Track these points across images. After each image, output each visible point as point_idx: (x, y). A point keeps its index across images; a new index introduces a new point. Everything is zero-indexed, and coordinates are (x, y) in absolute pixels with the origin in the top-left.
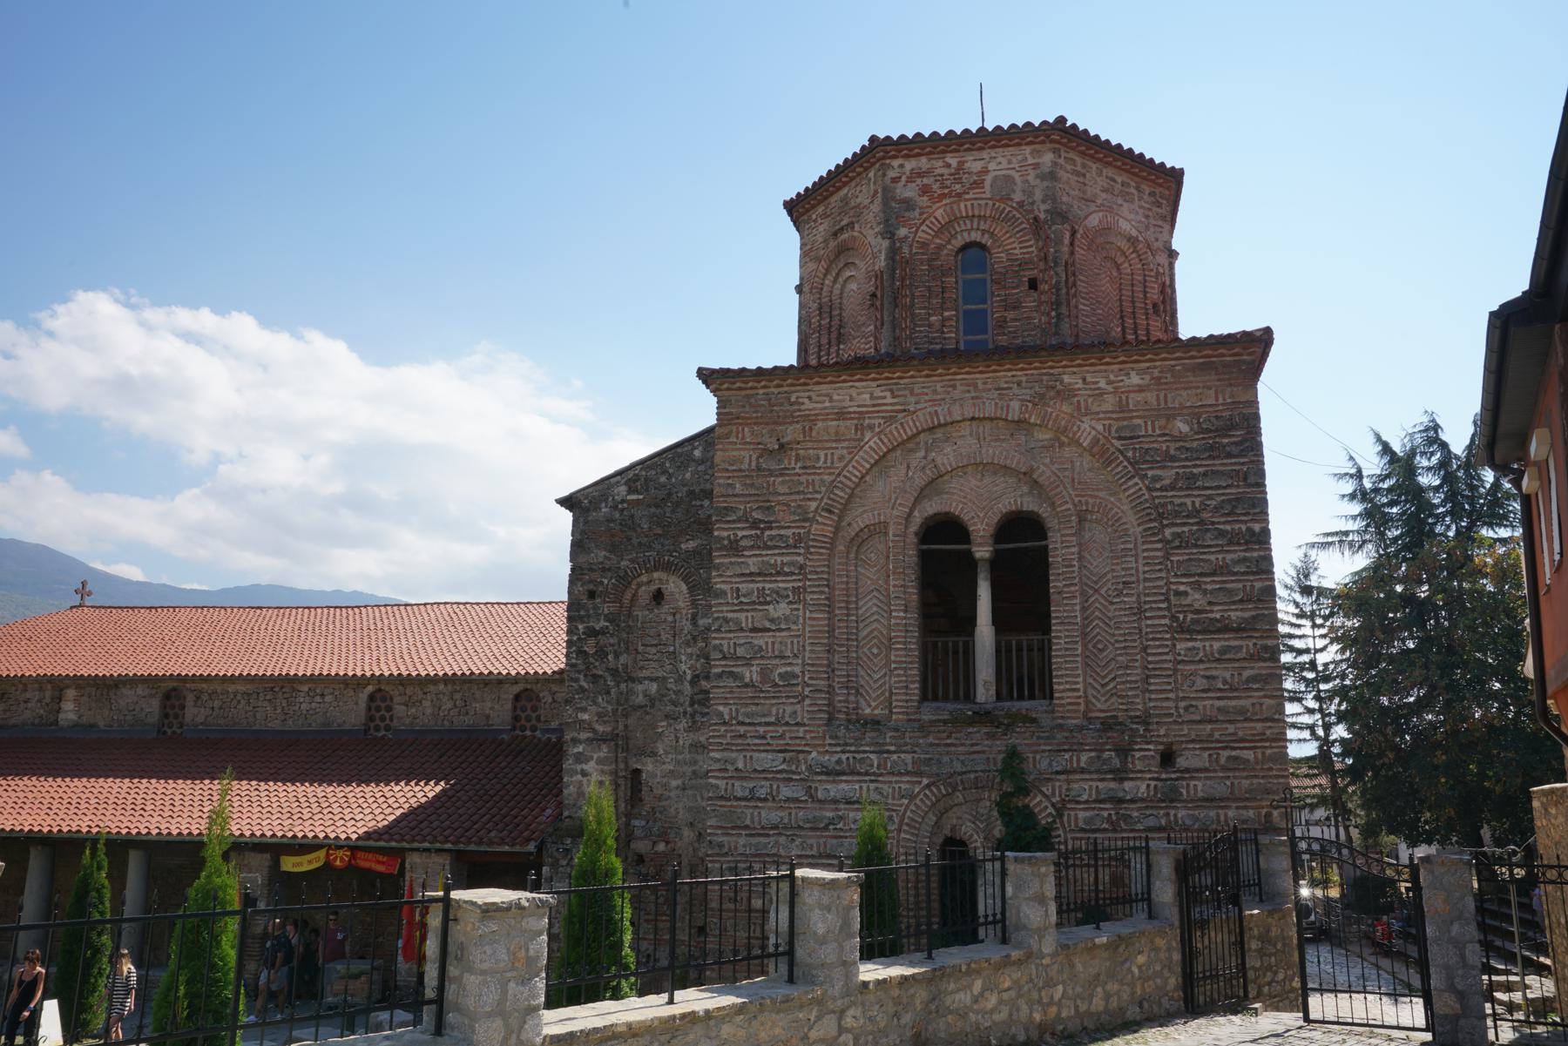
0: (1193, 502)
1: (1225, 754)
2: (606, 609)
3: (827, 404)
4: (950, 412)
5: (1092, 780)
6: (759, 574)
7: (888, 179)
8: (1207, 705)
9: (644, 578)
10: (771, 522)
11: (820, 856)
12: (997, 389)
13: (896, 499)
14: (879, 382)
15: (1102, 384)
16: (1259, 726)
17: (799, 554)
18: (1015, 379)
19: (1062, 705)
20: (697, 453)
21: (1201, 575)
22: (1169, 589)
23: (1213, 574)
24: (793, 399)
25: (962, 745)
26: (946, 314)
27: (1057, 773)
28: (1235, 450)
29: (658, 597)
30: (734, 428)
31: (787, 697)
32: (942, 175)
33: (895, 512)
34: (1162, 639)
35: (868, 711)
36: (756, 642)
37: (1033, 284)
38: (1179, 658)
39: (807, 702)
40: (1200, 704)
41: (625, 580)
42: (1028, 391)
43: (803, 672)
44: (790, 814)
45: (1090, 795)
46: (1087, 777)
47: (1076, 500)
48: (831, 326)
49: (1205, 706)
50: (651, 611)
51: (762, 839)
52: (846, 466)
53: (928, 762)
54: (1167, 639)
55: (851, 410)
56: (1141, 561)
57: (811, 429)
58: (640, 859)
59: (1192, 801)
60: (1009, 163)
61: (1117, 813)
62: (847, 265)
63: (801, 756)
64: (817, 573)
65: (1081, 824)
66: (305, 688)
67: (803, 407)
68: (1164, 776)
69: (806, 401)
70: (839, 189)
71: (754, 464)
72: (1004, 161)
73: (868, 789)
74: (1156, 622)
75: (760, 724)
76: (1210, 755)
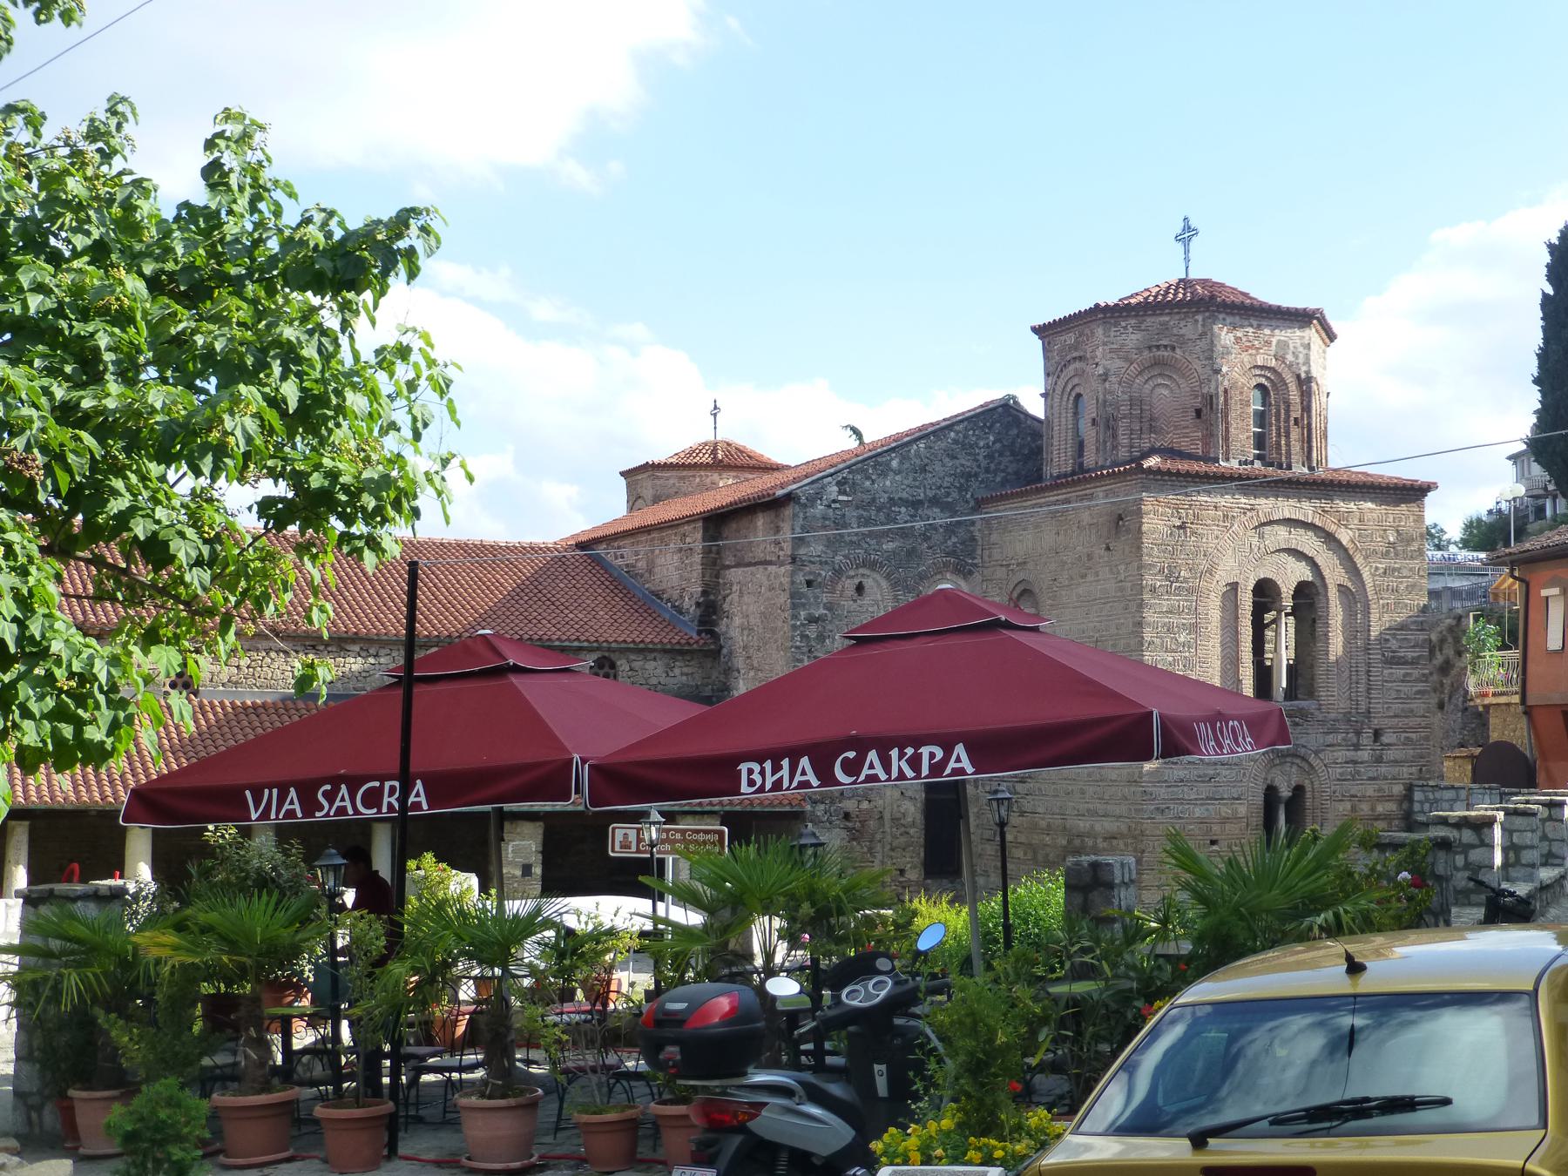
2: (825, 598)
8: (1397, 707)
9: (852, 573)
11: (1208, 798)
20: (895, 464)
29: (860, 589)
37: (1296, 419)
41: (838, 572)
50: (855, 601)
58: (847, 816)
66: (356, 648)
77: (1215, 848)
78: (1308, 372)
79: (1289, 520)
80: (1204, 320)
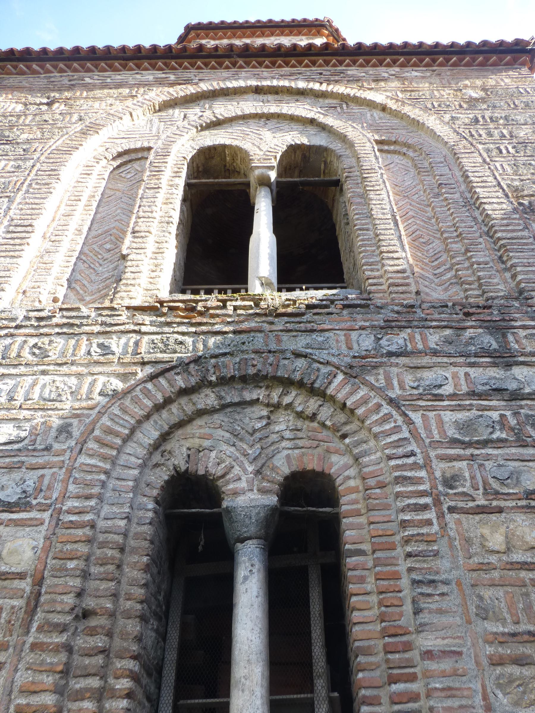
27: (390, 354)
65: (452, 432)
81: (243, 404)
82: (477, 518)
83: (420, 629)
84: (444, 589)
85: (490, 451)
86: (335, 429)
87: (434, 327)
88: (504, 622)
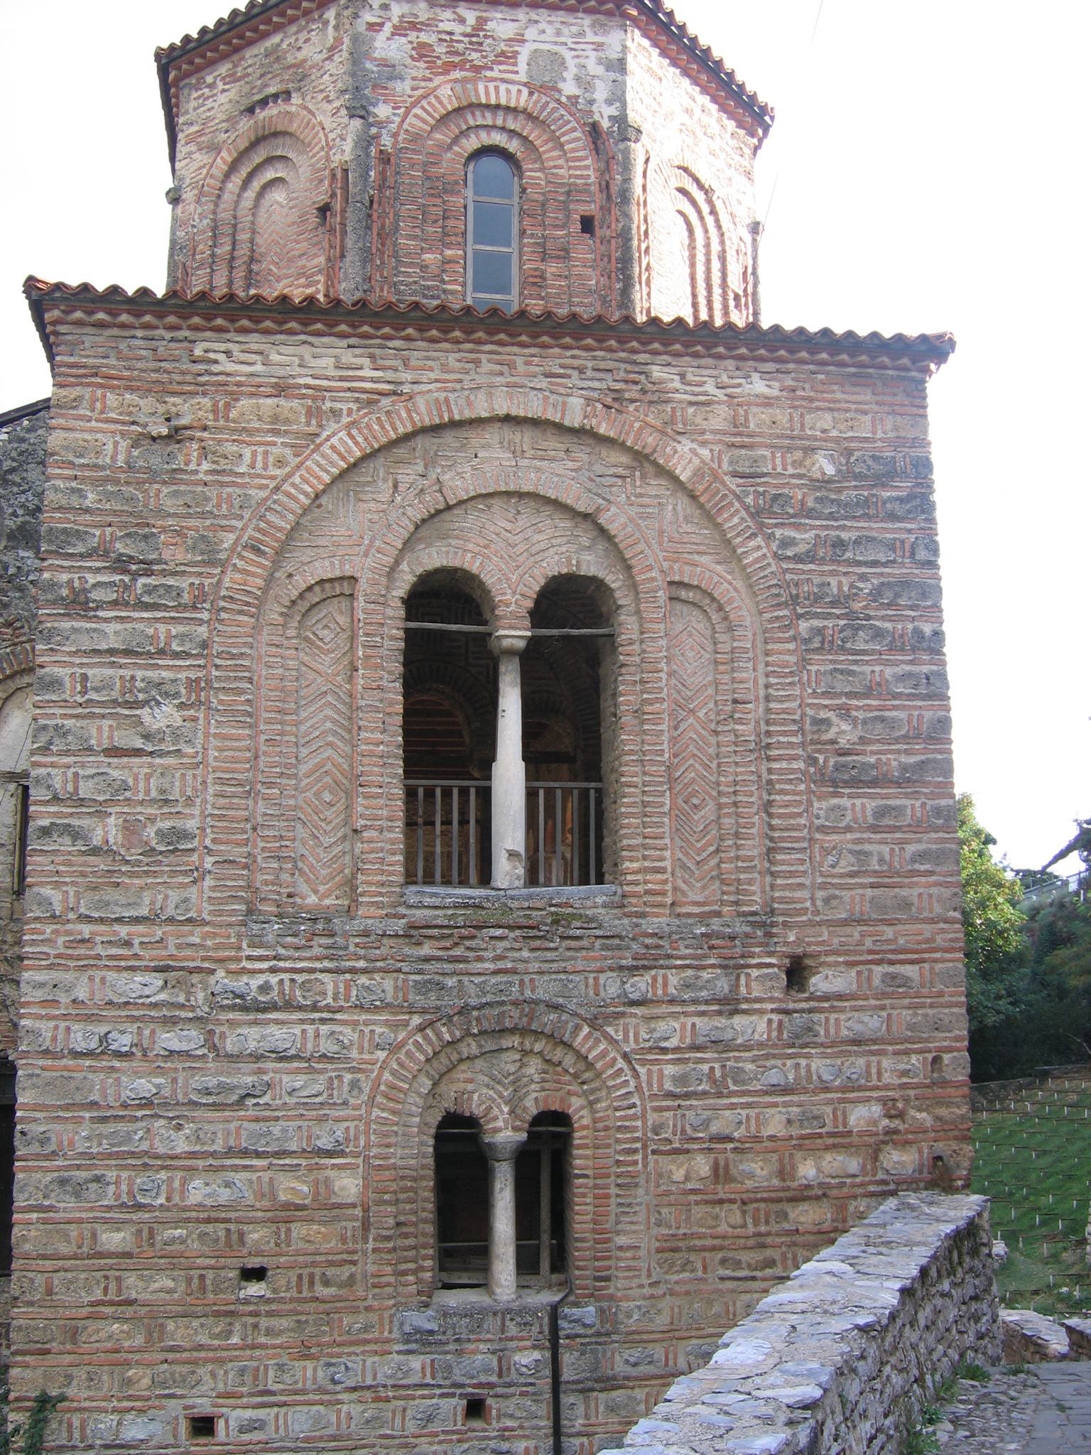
0: (840, 584)
1: (879, 970)
3: (259, 368)
4: (469, 403)
5: (685, 1014)
6: (127, 652)
7: (361, 27)
8: (856, 899)
10: (151, 563)
12: (547, 375)
13: (372, 541)
14: (352, 341)
15: (710, 387)
16: (927, 930)
17: (201, 622)
18: (576, 362)
19: (635, 895)
21: (849, 695)
22: (803, 715)
23: (867, 695)
24: (198, 352)
25: (480, 959)
26: (448, 252)
27: (633, 1003)
28: (899, 509)
30: (87, 392)
31: (174, 873)
32: (451, 33)
33: (369, 561)
34: (795, 793)
35: (312, 899)
36: (115, 774)
37: (587, 225)
38: (817, 822)
39: (209, 882)
40: (846, 895)
42: (596, 384)
43: (203, 829)
44: (174, 1080)
45: (682, 1039)
46: (678, 1009)
47: (666, 565)
48: (233, 259)
49: (852, 897)
51: (122, 1127)
52: (289, 475)
53: (422, 987)
54: (799, 793)
55: (301, 381)
56: (761, 667)
57: (228, 406)
59: (833, 1044)
60: (558, 33)
61: (724, 1066)
62: (270, 160)
63: (195, 978)
64: (233, 657)
65: (668, 1086)
67: (216, 368)
68: (791, 1006)
69: (221, 357)
70: (266, 35)
71: (121, 459)
72: (550, 30)
73: (317, 1036)
74: (784, 765)
75: (119, 920)
76: (859, 973)
77: (255, 1289)
78: (621, 120)
79: (508, 419)
80: (338, 15)
81: (501, 1050)
82: (670, 1157)
83: (618, 1233)
84: (637, 1208)
85: (694, 1103)
86: (576, 1076)
87: (676, 967)
88: (670, 1227)
